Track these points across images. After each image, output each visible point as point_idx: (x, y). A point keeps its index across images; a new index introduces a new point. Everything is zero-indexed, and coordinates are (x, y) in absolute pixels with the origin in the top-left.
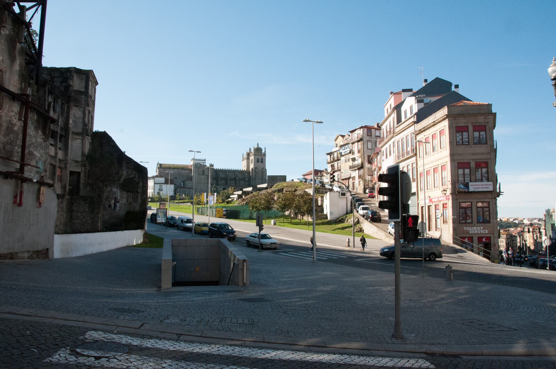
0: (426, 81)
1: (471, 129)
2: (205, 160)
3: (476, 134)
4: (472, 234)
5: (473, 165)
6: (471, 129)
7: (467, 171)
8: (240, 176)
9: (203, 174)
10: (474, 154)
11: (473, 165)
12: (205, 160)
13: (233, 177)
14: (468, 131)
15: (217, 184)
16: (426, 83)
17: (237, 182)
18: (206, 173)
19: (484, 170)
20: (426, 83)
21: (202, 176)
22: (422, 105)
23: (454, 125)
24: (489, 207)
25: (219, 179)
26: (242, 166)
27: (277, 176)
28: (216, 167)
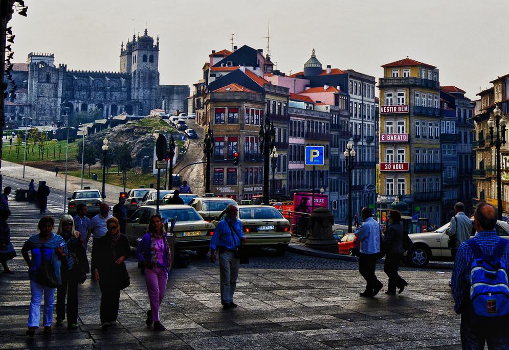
0: (235, 47)
1: (227, 111)
2: (52, 56)
3: (231, 115)
4: (222, 193)
5: (226, 139)
6: (227, 111)
7: (222, 144)
8: (114, 84)
9: (48, 81)
10: (228, 131)
11: (226, 139)
12: (52, 56)
13: (102, 85)
14: (224, 113)
15: (73, 98)
16: (236, 50)
17: (108, 94)
18: (53, 78)
19: (235, 143)
20: (236, 50)
21: (46, 85)
22: (214, 79)
23: (214, 108)
24: (236, 170)
25: (76, 88)
26: (114, 65)
27: (173, 87)
28: (69, 68)
